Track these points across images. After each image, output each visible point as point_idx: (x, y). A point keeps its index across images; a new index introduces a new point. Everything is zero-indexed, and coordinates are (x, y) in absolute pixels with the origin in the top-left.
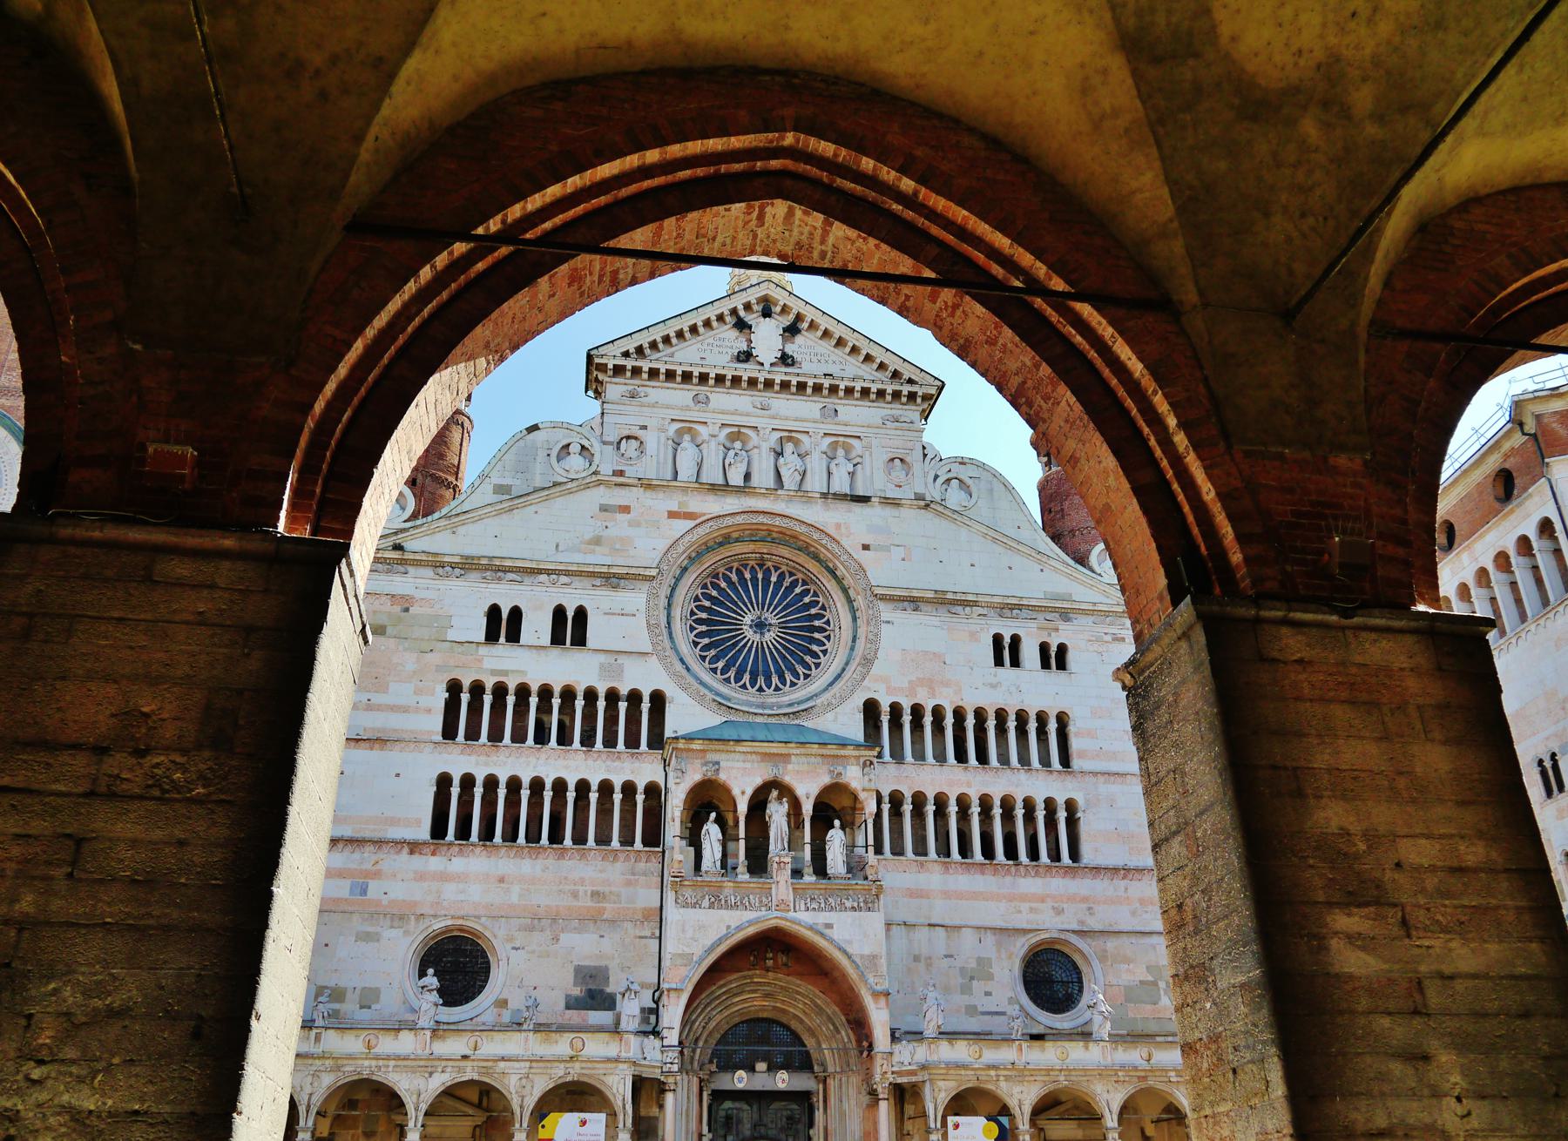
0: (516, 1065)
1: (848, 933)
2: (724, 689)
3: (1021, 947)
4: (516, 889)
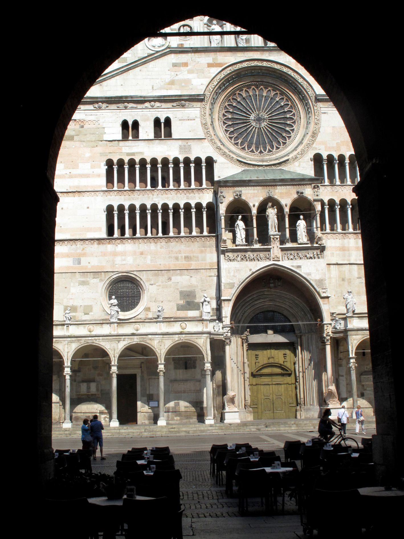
0: (157, 336)
1: (308, 269)
2: (242, 153)
4: (149, 257)
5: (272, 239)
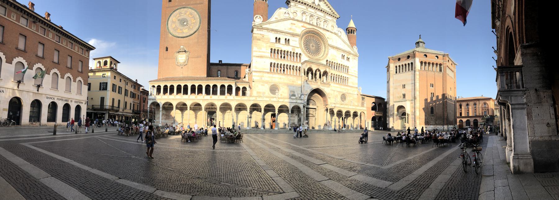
3: (341, 94)
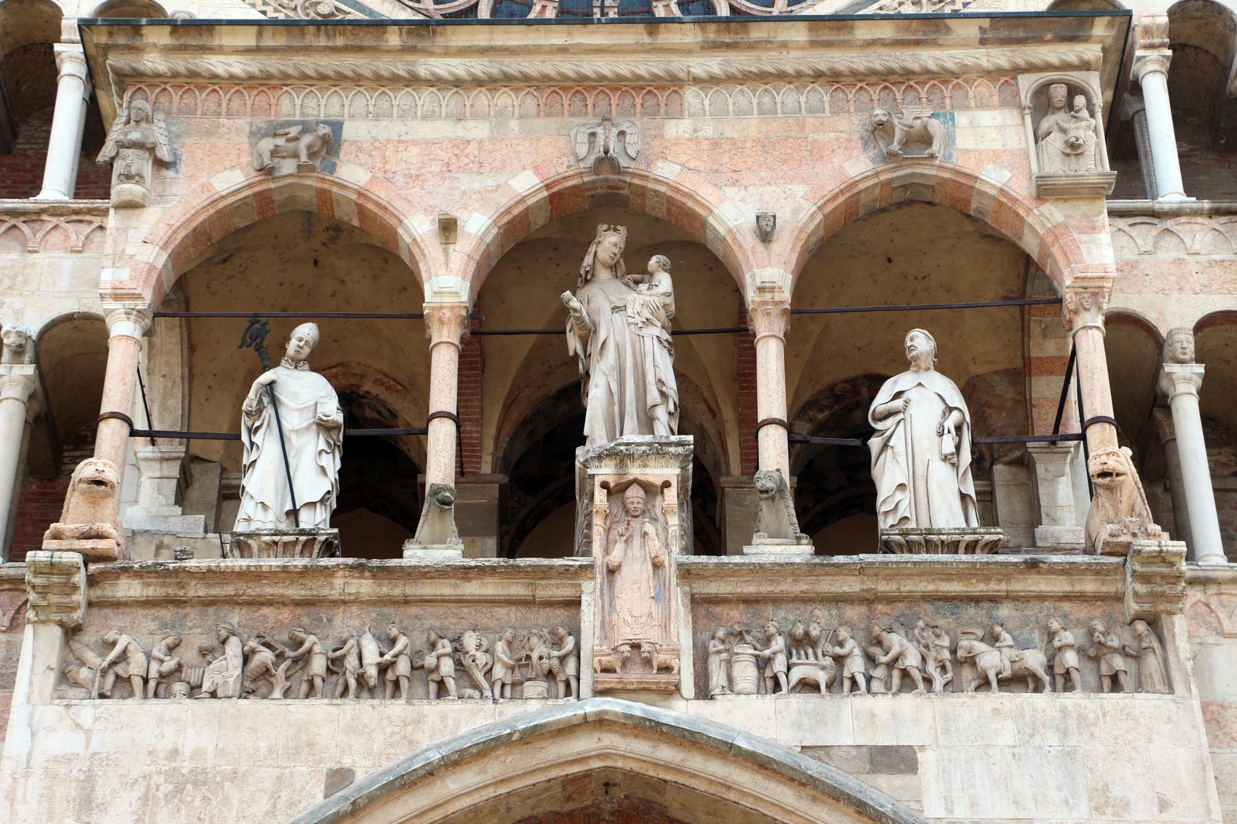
5: (600, 496)
